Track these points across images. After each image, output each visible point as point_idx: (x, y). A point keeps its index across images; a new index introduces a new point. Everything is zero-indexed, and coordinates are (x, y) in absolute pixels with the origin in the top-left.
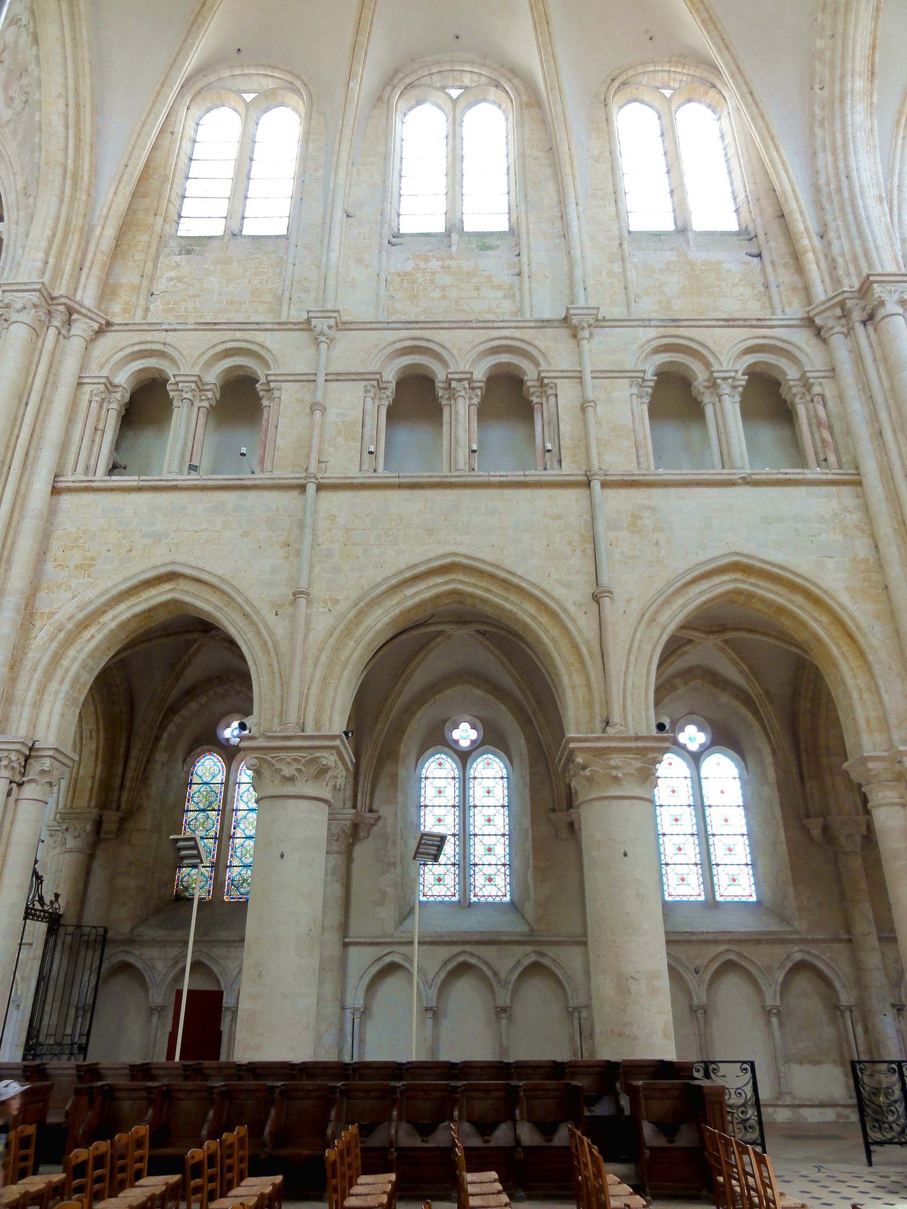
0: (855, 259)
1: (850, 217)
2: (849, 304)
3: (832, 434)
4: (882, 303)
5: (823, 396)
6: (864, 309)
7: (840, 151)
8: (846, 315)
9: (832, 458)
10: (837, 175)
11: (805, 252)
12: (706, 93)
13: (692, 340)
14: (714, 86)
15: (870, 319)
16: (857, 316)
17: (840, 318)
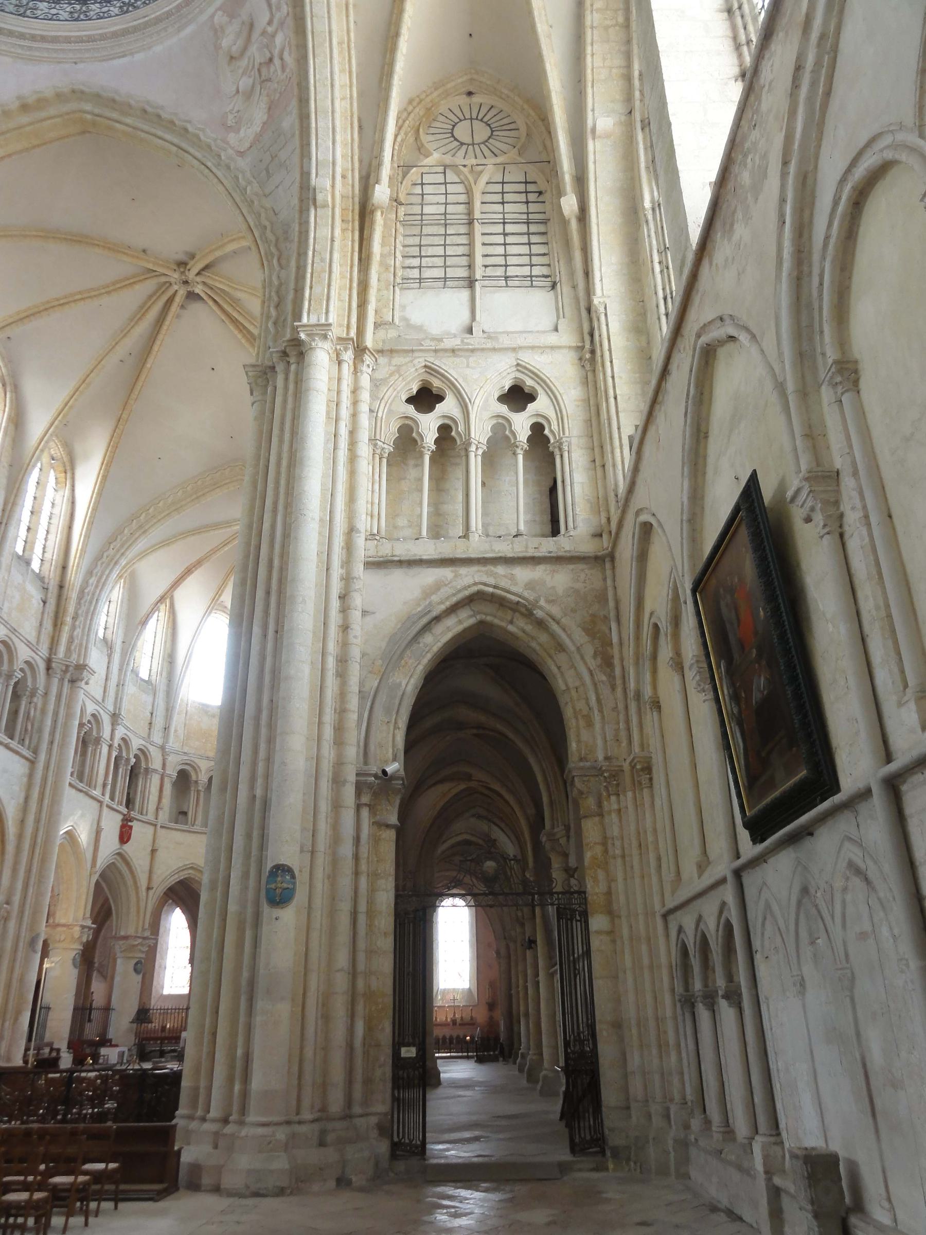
0: (81, 645)
1: (88, 622)
2: (71, 668)
3: (32, 727)
4: (82, 680)
5: (36, 704)
6: (72, 674)
7: (101, 585)
8: (65, 672)
9: (27, 742)
10: (93, 594)
11: (65, 625)
12: (61, 472)
13: (14, 644)
14: (66, 472)
15: (73, 681)
16: (68, 676)
17: (62, 671)
